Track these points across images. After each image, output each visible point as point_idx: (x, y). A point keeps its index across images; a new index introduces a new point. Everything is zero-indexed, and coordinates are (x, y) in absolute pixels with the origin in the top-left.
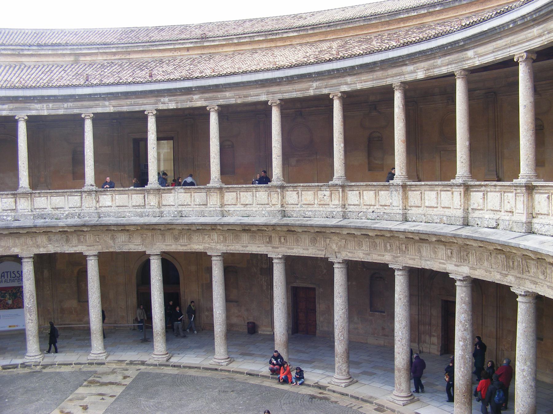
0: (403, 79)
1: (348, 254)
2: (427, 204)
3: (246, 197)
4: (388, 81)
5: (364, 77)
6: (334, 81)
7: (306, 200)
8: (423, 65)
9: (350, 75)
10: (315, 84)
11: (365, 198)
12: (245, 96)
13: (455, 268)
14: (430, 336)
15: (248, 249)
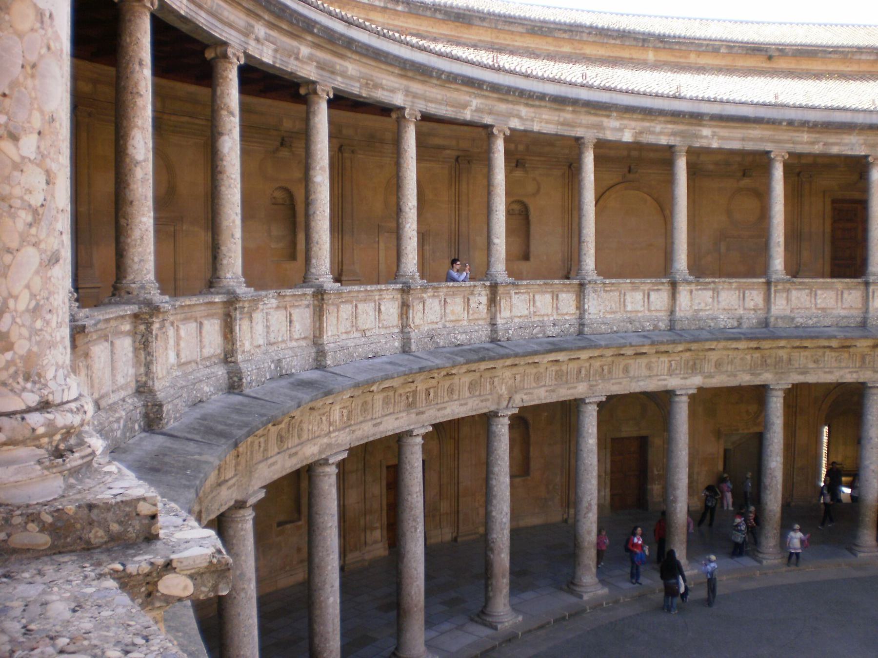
0: (601, 136)
1: (525, 397)
2: (629, 308)
3: (367, 313)
4: (579, 132)
5: (546, 115)
6: (503, 107)
7: (453, 312)
8: (633, 124)
9: (527, 105)
10: (475, 102)
11: (538, 304)
12: (377, 86)
13: (682, 382)
14: (373, 529)
15: (381, 428)
